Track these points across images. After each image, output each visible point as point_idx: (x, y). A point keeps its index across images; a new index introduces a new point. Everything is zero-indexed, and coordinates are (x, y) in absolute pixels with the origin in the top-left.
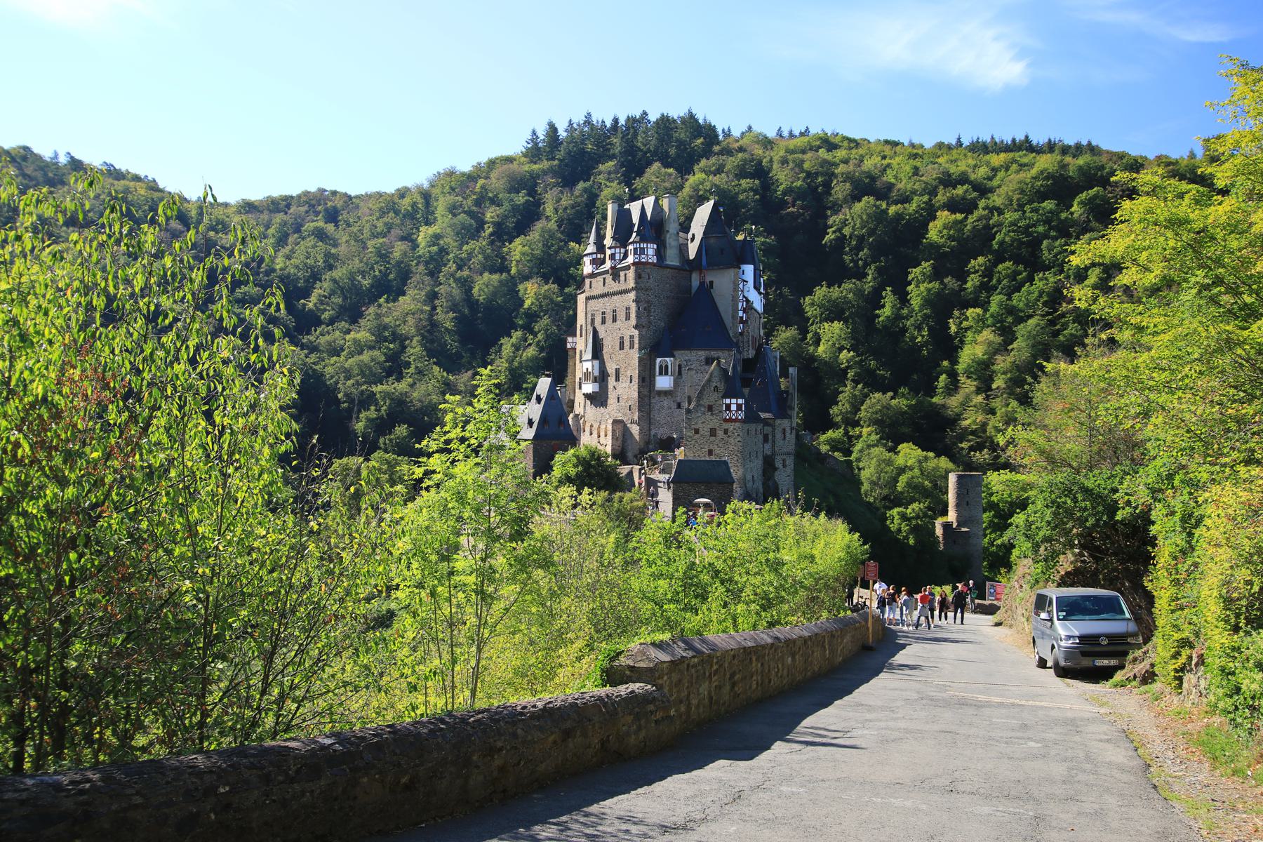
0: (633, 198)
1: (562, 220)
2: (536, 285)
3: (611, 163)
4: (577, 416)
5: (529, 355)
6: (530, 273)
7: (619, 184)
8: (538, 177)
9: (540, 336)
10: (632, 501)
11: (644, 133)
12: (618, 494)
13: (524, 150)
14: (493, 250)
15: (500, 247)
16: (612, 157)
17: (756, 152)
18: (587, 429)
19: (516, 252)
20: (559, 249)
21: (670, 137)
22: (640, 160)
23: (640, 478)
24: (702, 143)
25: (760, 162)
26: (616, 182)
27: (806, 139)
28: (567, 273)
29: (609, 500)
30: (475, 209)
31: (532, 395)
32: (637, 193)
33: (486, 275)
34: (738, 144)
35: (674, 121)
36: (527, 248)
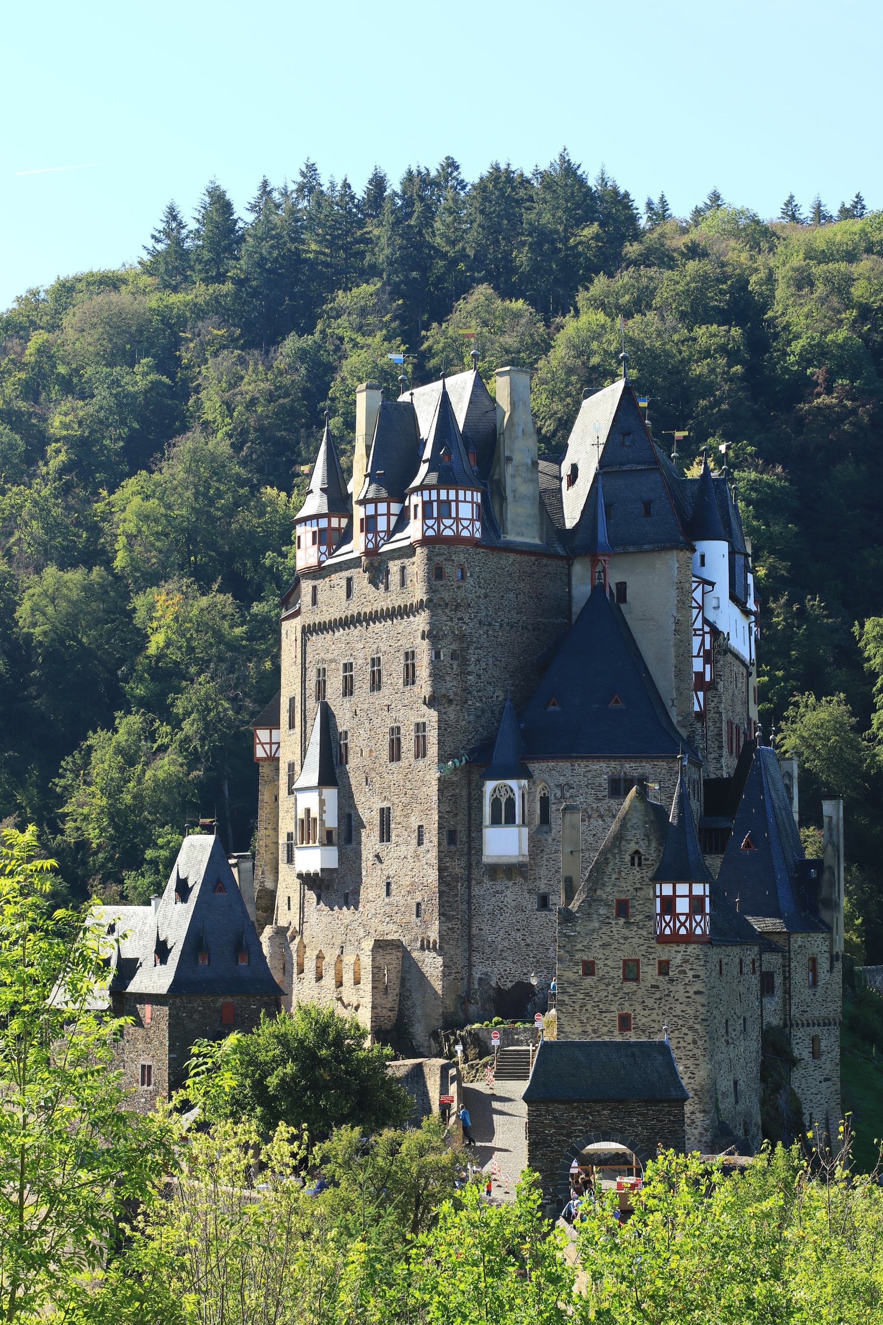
0: (423, 377)
1: (244, 432)
2: (178, 597)
3: (366, 289)
4: (281, 932)
5: (161, 775)
6: (163, 564)
7: (387, 338)
8: (182, 322)
9: (189, 727)
10: (422, 1151)
11: (450, 211)
12: (388, 1133)
13: (146, 257)
14: (68, 508)
15: (88, 502)
16: (370, 273)
17: (731, 256)
18: (310, 965)
19: (128, 514)
20: (236, 504)
21: (515, 221)
22: (440, 279)
23: (444, 1090)
24: (597, 237)
25: (742, 283)
26: (379, 335)
27: (856, 225)
28: (257, 564)
29: (365, 1151)
30: (22, 405)
31: (167, 877)
32: (433, 362)
33: (51, 571)
34: (686, 239)
35: (525, 182)
36: (153, 503)
